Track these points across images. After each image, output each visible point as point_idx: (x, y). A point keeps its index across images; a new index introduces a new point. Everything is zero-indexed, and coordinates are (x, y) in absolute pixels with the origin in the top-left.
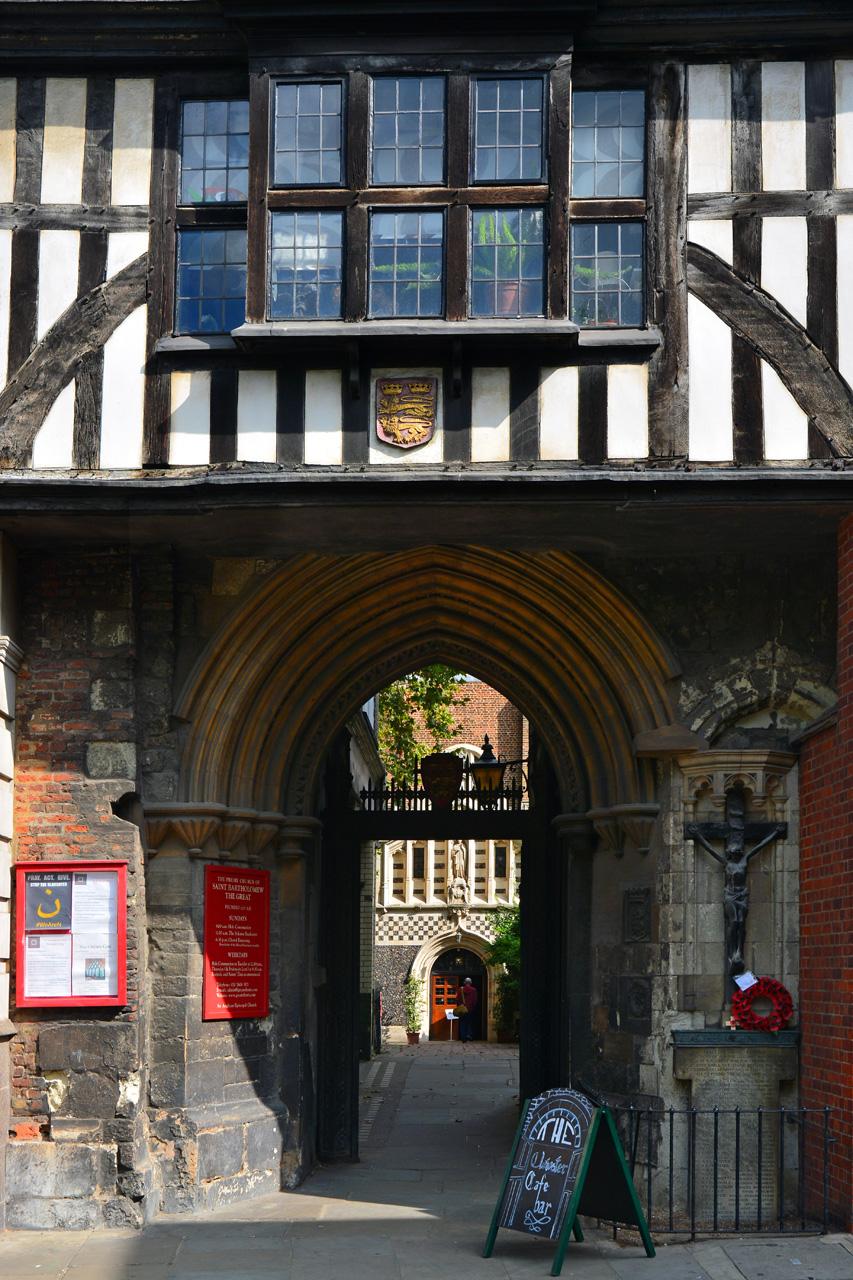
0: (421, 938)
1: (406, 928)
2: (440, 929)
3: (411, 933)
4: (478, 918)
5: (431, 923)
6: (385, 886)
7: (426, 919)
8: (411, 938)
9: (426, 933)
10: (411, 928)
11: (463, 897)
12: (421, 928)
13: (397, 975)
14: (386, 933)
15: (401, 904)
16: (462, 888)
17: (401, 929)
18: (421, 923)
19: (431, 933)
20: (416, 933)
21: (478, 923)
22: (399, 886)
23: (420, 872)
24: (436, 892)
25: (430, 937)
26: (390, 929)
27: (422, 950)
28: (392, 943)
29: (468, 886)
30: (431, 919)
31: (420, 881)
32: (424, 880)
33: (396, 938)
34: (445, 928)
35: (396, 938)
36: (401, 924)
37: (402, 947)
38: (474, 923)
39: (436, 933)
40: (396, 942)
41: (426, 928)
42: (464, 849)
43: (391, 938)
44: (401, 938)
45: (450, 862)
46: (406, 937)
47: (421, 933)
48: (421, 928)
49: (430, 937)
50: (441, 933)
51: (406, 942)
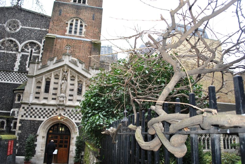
0: (44, 117)
1: (38, 113)
2: (52, 114)
3: (40, 115)
4: (69, 111)
6: (31, 94)
7: (47, 110)
8: (40, 117)
9: (46, 115)
10: (40, 113)
11: (63, 101)
12: (44, 113)
14: (29, 114)
16: (63, 97)
18: (45, 111)
19: (48, 115)
20: (42, 115)
21: (68, 113)
22: (37, 95)
23: (47, 90)
25: (48, 117)
26: (31, 113)
29: (66, 97)
30: (49, 109)
31: (47, 94)
33: (33, 117)
34: (54, 114)
35: (33, 117)
36: (36, 111)
38: (67, 113)
40: (33, 118)
41: (46, 113)
43: (31, 117)
44: (35, 117)
46: (37, 117)
47: (44, 115)
50: (52, 116)
51: (37, 119)
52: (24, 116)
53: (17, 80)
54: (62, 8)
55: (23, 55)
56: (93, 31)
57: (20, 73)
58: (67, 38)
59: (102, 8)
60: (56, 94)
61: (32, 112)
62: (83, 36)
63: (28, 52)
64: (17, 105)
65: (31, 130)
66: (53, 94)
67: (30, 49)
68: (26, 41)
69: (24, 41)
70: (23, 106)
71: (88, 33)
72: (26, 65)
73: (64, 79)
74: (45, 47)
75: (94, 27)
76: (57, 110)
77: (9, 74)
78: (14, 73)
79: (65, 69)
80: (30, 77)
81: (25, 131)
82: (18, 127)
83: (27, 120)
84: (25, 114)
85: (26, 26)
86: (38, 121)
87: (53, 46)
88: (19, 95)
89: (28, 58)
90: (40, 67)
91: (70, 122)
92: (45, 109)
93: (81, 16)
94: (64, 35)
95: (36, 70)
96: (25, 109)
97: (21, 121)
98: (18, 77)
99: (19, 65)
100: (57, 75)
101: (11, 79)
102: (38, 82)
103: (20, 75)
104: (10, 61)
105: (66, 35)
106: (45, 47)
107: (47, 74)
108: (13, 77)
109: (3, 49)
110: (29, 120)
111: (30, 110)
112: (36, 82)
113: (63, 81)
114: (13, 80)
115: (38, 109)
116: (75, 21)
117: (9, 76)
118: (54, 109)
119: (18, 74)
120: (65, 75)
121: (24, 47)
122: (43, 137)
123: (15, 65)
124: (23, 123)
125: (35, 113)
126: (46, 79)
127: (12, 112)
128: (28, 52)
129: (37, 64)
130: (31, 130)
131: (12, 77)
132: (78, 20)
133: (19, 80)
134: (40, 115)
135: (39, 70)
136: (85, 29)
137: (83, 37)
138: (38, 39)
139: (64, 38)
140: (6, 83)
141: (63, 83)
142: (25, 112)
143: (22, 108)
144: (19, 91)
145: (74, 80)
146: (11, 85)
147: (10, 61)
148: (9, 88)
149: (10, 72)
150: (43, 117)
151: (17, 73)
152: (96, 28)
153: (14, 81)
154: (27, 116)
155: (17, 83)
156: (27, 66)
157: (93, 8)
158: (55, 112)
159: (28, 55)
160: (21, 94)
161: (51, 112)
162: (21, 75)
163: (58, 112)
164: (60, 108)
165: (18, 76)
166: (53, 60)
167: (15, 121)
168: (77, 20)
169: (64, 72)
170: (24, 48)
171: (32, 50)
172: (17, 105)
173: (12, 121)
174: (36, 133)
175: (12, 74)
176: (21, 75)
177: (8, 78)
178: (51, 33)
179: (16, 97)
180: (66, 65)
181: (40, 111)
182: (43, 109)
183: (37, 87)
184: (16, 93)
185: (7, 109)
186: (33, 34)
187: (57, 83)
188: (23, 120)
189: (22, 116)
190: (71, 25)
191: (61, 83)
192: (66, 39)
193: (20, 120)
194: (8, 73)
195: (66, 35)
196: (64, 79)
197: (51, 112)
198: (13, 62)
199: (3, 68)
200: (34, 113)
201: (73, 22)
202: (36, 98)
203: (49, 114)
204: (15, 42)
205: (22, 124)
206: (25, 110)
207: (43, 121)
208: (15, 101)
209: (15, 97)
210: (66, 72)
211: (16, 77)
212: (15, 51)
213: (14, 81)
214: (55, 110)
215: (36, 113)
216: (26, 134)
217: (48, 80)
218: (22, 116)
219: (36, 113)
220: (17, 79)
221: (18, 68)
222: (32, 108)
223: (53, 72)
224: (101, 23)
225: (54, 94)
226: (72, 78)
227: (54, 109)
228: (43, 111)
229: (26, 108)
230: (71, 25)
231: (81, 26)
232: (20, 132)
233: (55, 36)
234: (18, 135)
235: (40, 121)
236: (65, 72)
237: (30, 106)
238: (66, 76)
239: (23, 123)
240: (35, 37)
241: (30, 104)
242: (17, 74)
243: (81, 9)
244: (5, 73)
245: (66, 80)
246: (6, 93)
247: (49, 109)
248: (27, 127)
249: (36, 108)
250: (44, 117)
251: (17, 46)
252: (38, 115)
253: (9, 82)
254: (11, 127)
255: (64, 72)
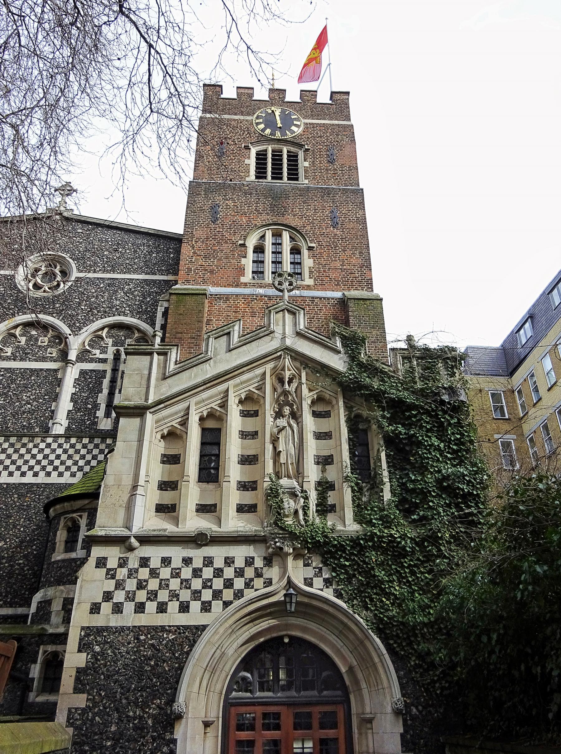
0: (206, 607)
1: (175, 584)
2: (248, 584)
5: (229, 573)
6: (140, 490)
7: (219, 563)
8: (184, 608)
9: (217, 595)
10: (186, 584)
12: (207, 584)
13: (145, 705)
14: (131, 597)
15: (170, 528)
17: (164, 584)
18: (208, 573)
19: (228, 595)
20: (197, 595)
22: (168, 497)
24: (241, 509)
25: (226, 604)
26: (141, 585)
27: (206, 636)
28: (142, 620)
30: (229, 561)
31: (211, 486)
32: (220, 486)
33: (151, 607)
34: (258, 583)
36: (165, 573)
37: (163, 628)
39: (239, 594)
42: (295, 426)
43: (140, 608)
44: (162, 608)
45: (269, 448)
46: (173, 606)
48: (207, 584)
49: (226, 604)
50: (250, 594)
52: (106, 608)
53: (62, 469)
54: (219, 199)
55: (83, 373)
56: (338, 264)
57: (73, 440)
58: (249, 295)
59: (361, 187)
60: (255, 482)
61: (146, 581)
62: (309, 281)
63: (104, 361)
64: (63, 570)
65: (143, 689)
66: (239, 482)
67: (111, 350)
68: (94, 322)
69: (87, 322)
70: (97, 552)
71: (324, 271)
72: (96, 407)
73: (287, 410)
74: (171, 330)
75: (344, 251)
76: (268, 562)
77: (31, 445)
78: (49, 440)
79: (283, 369)
80: (132, 411)
81: (111, 696)
82: (74, 673)
83: (121, 630)
84: (108, 596)
85: (95, 272)
86: (178, 627)
87: (200, 321)
88: (70, 524)
89: (106, 382)
90: (172, 367)
91: (342, 622)
92: (208, 562)
93: (290, 220)
94: (237, 286)
95: (157, 379)
96: (109, 570)
97: (87, 635)
98: (64, 457)
99: (69, 411)
100: (248, 399)
101: (37, 468)
102: (165, 432)
103: (72, 446)
104: (34, 400)
105: (245, 285)
106: (171, 330)
107: (205, 395)
108: (46, 457)
109: (9, 354)
110: (128, 628)
111: (136, 571)
112: (159, 436)
113: (282, 422)
114: (44, 468)
115: (176, 563)
116: (269, 235)
117: (27, 457)
118: (253, 558)
119: (66, 446)
120: (286, 393)
121: (89, 345)
122: (207, 724)
123: (53, 412)
124: (97, 649)
125: (160, 587)
126: (201, 419)
127: (38, 607)
128: (104, 361)
129: (159, 354)
130: (143, 689)
131: (40, 457)
132: (280, 235)
133: (68, 468)
134: (185, 595)
135: (169, 380)
136: (312, 260)
137: (308, 287)
138: (139, 313)
139: (237, 295)
140: (14, 484)
141: (284, 428)
142: (110, 585)
143: (92, 561)
144: (72, 502)
145: (326, 415)
146: (33, 492)
147: (34, 400)
148: (27, 506)
149: (32, 437)
150: (203, 603)
151: (61, 440)
152: (348, 253)
153: (48, 474)
154: (118, 609)
155: (62, 480)
156: (100, 413)
157: (327, 192)
158: (259, 574)
159: (105, 371)
160: (81, 516)
161: (240, 573)
162: (78, 446)
163: (273, 573)
164: (286, 549)
165: (65, 451)
166: (229, 334)
167: (50, 648)
168: (277, 235)
169: (281, 380)
170: (87, 347)
171: (118, 351)
172: (61, 568)
173: (38, 652)
174: (172, 700)
175: (43, 445)
176: (78, 446)
177: (26, 462)
178: (188, 281)
179: (59, 533)
180: (287, 350)
181: (187, 573)
182: (198, 563)
183: (164, 456)
184: (58, 516)
185: (15, 597)
186: (121, 294)
187: (254, 435)
188: (100, 631)
189: (95, 609)
190: (259, 249)
191: (275, 430)
192: (245, 296)
193: (83, 628)
194: (24, 445)
195: (245, 285)
196: (287, 410)
197: (240, 573)
198: (44, 399)
199: (7, 427)
200: (153, 584)
201: (264, 241)
202: (161, 509)
203: (229, 584)
204: (54, 328)
205: (95, 656)
206: (111, 574)
207: (204, 627)
208: (54, 550)
209: (55, 535)
210: (290, 381)
211: (58, 457)
212: (55, 361)
213: (48, 474)
214: (259, 563)
215: (164, 584)
216: (117, 710)
217: (211, 424)
218: (95, 609)
219: (168, 586)
220: (63, 463)
221: (65, 423)
222: (144, 562)
223: (231, 382)
224: (365, 236)
225: (244, 486)
226: (320, 408)
227: (253, 558)
228: (201, 570)
229: (112, 563)
230: (259, 249)
231: (295, 251)
232: (81, 701)
233: (205, 290)
234: (70, 722)
235: (186, 627)
236: (287, 380)
237: (131, 549)
238: (290, 398)
239: (97, 649)
240: (129, 306)
241: (133, 540)
242: (60, 446)
243: (287, 198)
244: (12, 445)
245: (295, 416)
246: (15, 526)
247: (229, 561)
248: (117, 672)
249: (166, 561)
250: (206, 607)
251: (60, 343)
252: (174, 595)
253: (29, 479)
254: (27, 686)
255: (281, 380)
